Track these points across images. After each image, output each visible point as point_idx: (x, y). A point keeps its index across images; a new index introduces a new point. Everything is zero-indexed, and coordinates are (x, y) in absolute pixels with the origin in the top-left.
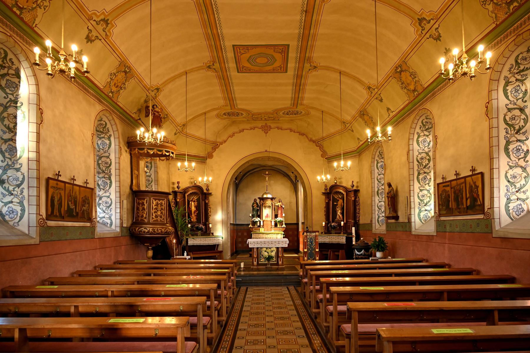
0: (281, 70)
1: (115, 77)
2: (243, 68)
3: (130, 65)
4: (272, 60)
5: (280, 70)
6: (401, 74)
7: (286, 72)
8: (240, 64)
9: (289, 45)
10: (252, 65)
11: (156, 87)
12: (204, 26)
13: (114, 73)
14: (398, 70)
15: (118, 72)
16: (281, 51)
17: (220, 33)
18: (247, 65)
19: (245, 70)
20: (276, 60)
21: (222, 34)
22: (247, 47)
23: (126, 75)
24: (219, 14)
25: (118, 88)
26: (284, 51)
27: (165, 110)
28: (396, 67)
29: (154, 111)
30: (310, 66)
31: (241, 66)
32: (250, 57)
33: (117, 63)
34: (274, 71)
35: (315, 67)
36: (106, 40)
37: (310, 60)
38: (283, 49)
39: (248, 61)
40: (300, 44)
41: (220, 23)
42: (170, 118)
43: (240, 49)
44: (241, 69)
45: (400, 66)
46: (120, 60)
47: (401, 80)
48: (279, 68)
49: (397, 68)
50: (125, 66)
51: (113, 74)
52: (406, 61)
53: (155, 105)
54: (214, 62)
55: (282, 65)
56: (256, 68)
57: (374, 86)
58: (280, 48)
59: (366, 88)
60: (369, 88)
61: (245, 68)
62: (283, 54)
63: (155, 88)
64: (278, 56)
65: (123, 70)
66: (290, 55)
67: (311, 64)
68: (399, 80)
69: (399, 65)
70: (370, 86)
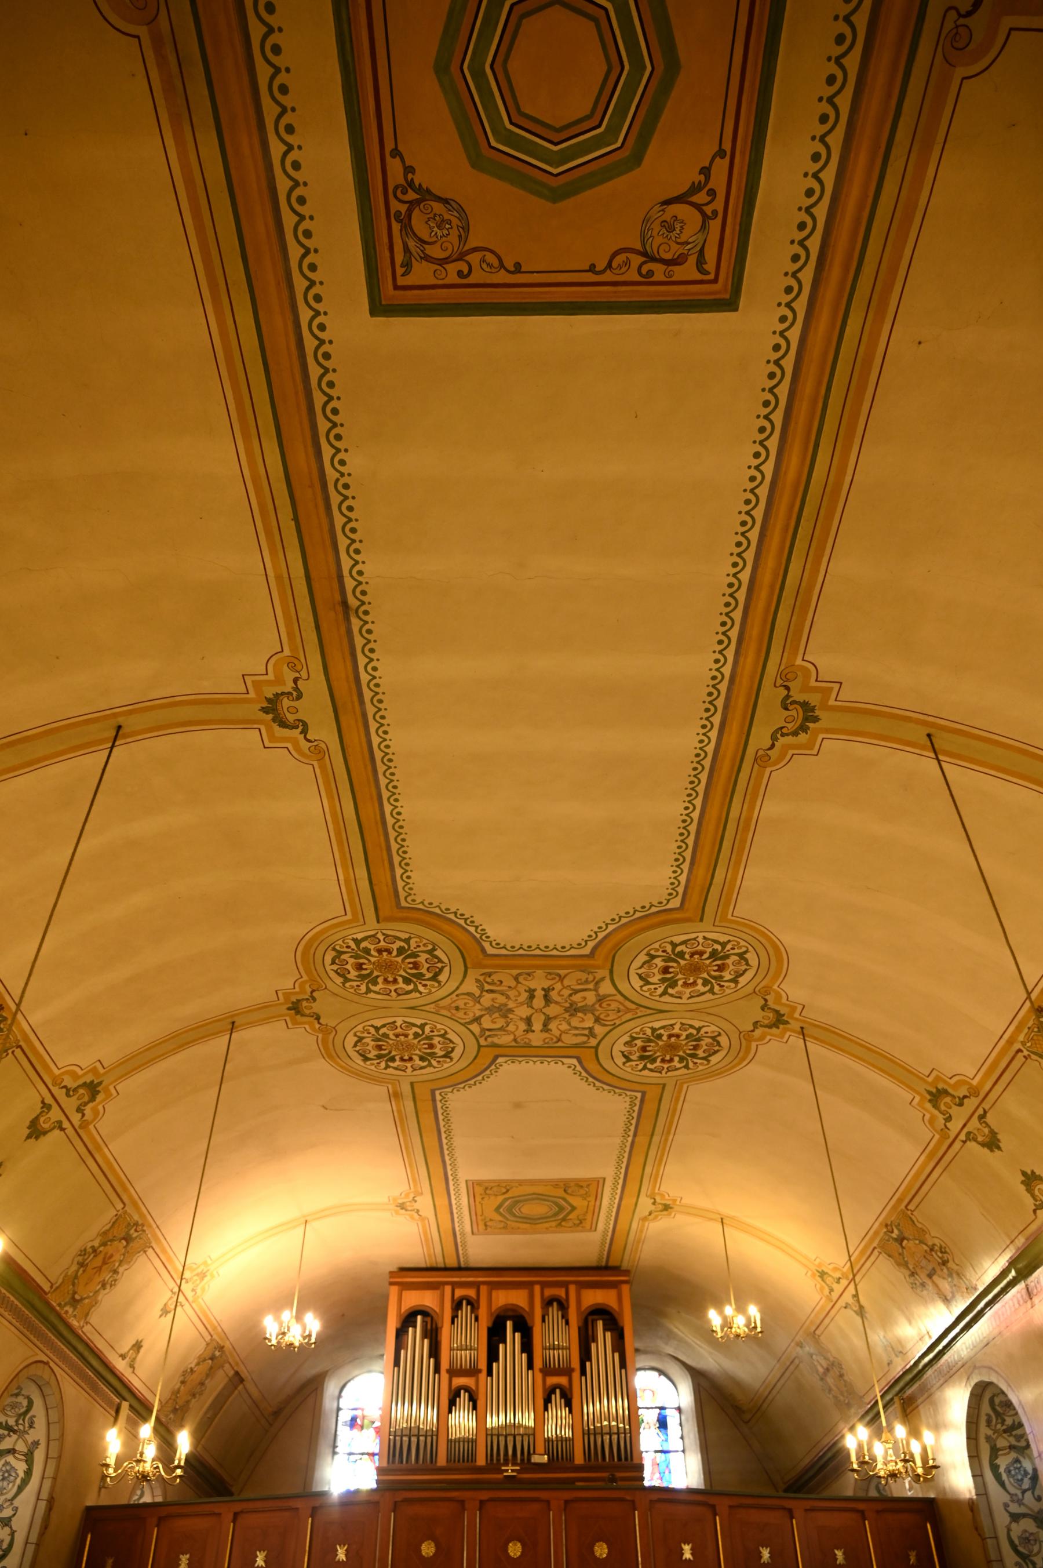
16: (418, 221)
26: (396, 227)
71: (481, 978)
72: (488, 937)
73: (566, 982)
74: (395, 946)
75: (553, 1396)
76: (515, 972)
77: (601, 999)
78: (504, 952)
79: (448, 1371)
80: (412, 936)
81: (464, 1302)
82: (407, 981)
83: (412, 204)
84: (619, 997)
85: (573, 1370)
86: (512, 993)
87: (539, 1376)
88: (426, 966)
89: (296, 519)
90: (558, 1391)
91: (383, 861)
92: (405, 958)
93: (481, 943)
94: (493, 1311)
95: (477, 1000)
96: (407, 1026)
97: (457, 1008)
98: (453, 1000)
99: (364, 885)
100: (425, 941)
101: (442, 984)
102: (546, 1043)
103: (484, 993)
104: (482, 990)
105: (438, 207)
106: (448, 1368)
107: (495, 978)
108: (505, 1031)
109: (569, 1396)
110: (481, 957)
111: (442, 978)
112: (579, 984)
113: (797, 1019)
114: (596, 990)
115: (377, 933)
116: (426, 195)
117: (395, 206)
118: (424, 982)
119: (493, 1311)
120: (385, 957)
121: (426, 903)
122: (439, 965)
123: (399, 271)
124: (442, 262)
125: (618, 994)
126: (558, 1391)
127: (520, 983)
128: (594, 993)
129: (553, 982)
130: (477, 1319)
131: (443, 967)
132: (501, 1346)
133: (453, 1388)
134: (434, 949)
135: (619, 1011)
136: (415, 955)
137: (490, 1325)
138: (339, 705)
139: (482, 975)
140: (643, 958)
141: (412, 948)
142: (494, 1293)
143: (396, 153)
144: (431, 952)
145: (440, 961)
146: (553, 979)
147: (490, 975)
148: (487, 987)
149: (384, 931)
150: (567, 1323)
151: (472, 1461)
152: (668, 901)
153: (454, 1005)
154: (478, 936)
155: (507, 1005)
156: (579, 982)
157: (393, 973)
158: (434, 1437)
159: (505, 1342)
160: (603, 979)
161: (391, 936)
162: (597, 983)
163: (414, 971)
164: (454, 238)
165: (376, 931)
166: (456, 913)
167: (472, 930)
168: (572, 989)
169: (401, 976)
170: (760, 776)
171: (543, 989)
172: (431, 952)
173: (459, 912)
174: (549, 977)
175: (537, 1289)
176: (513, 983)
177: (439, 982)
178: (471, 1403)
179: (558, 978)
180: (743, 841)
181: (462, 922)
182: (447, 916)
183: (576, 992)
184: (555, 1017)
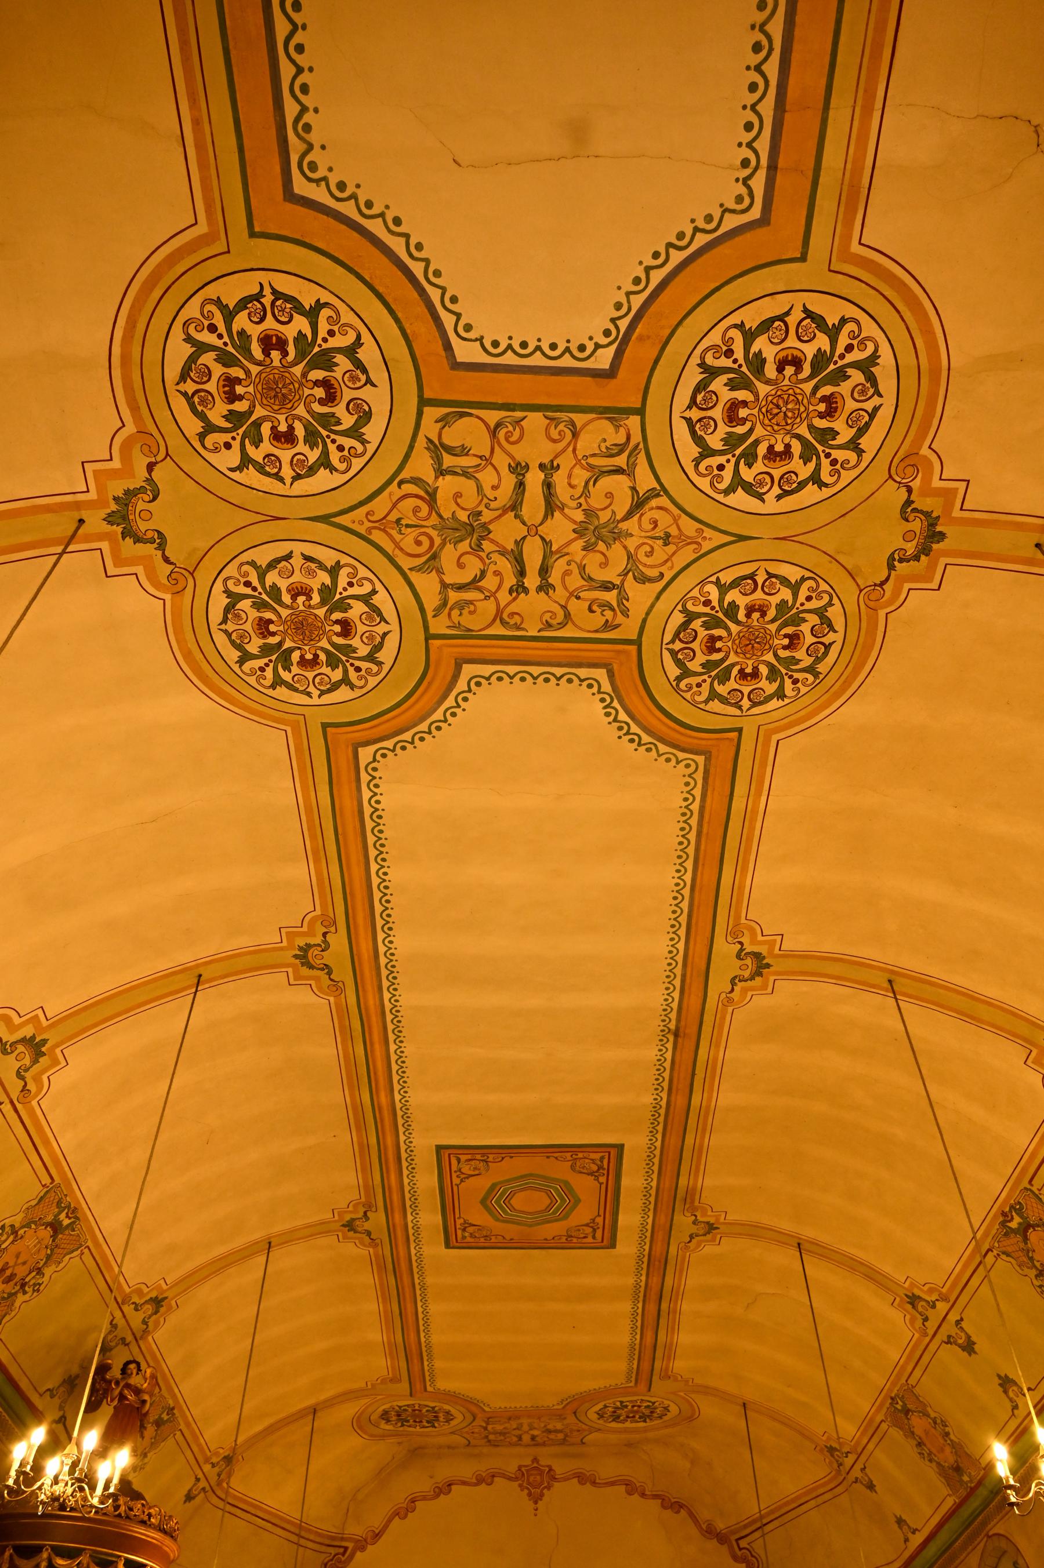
0: (594, 1237)
1: (12, 1242)
2: (464, 1230)
3: (78, 1202)
4: (562, 1198)
5: (590, 1239)
6: (1026, 1239)
7: (613, 1245)
8: (457, 1215)
9: (622, 1146)
10: (497, 1220)
11: (154, 1295)
12: (352, 1082)
13: (12, 1226)
14: (1014, 1225)
15: (28, 1225)
16: (595, 1168)
17: (398, 1105)
18: (478, 1217)
19: (471, 1235)
20: (580, 1200)
21: (405, 1107)
22: (485, 1154)
23: (54, 1236)
24: (401, 1042)
25: (12, 1283)
26: (606, 1166)
27: (170, 1390)
28: (1004, 1214)
29: (122, 1384)
30: (694, 1223)
31: (459, 1222)
32: (493, 1187)
33: (37, 1190)
34: (569, 1241)
35: (711, 1228)
36: (19, 1106)
37: (693, 1202)
38: (602, 1158)
39: (483, 1202)
40: (658, 1144)
41: (404, 1072)
42: (182, 1426)
43: (459, 1161)
44: (459, 1232)
45: (1018, 1208)
46: (46, 1180)
47: (1031, 1259)
48: (589, 1230)
49: (1006, 1216)
50: (59, 1202)
51: (7, 1229)
52: (1034, 1189)
53: (134, 1361)
54: (369, 1207)
55: (600, 1220)
56: (511, 1231)
57: (931, 1291)
58: (593, 1156)
59: (902, 1300)
60: (913, 1300)
61: (471, 1229)
62: (603, 1179)
63: (148, 1298)
64: (585, 1187)
65: (50, 1218)
66: (625, 1182)
67: (698, 1214)
68: (1025, 1259)
69: (1012, 1207)
70: (917, 1292)
71: (620, 618)
72: (603, 700)
73: (490, 607)
74: (732, 684)
76: (567, 632)
77: (432, 561)
78: (583, 672)
80: (702, 706)
82: (731, 611)
83: (597, 1172)
84: (406, 563)
86: (575, 581)
88: (695, 646)
89: (693, 1074)
91: (709, 823)
92: (723, 660)
93: (614, 690)
95: (633, 568)
96: (761, 484)
97: (667, 539)
98: (669, 564)
99: (741, 789)
100: (688, 696)
101: (680, 607)
102: (518, 422)
103: (617, 581)
104: (621, 588)
105: (585, 1171)
107: (598, 620)
108: (591, 467)
110: (615, 667)
111: (678, 618)
112: (471, 602)
113: (100, 537)
114: (444, 586)
115: (749, 709)
116: (591, 1174)
117: (605, 1172)
118: (707, 610)
120: (750, 663)
121: (673, 762)
122: (678, 646)
123: (607, 1157)
124: (585, 1158)
125: (408, 572)
127: (562, 606)
128: (448, 580)
129: (513, 608)
131: (673, 641)
134: (679, 679)
135: (398, 521)
136: (708, 666)
138: (702, 979)
139: (618, 626)
140: (386, 655)
141: (709, 680)
143: (601, 1184)
144: (686, 673)
145: (674, 654)
146: (512, 615)
147: (607, 626)
148: (611, 597)
149: (738, 712)
152: (374, 760)
153: (671, 548)
154: (616, 704)
155: (584, 549)
156: (472, 608)
157: (749, 627)
160: (437, 614)
161: (731, 705)
162: (445, 603)
163: (717, 632)
164: (578, 1164)
165: (749, 713)
166: (639, 744)
167: (623, 716)
168: (480, 589)
169: (738, 623)
170: (324, 905)
171: (526, 591)
172: (686, 673)
173: (635, 745)
174: (517, 619)
176: (574, 605)
177: (684, 611)
179: (505, 616)
180: (313, 837)
181: (634, 728)
182: (651, 740)
183: (473, 584)
184: (505, 511)
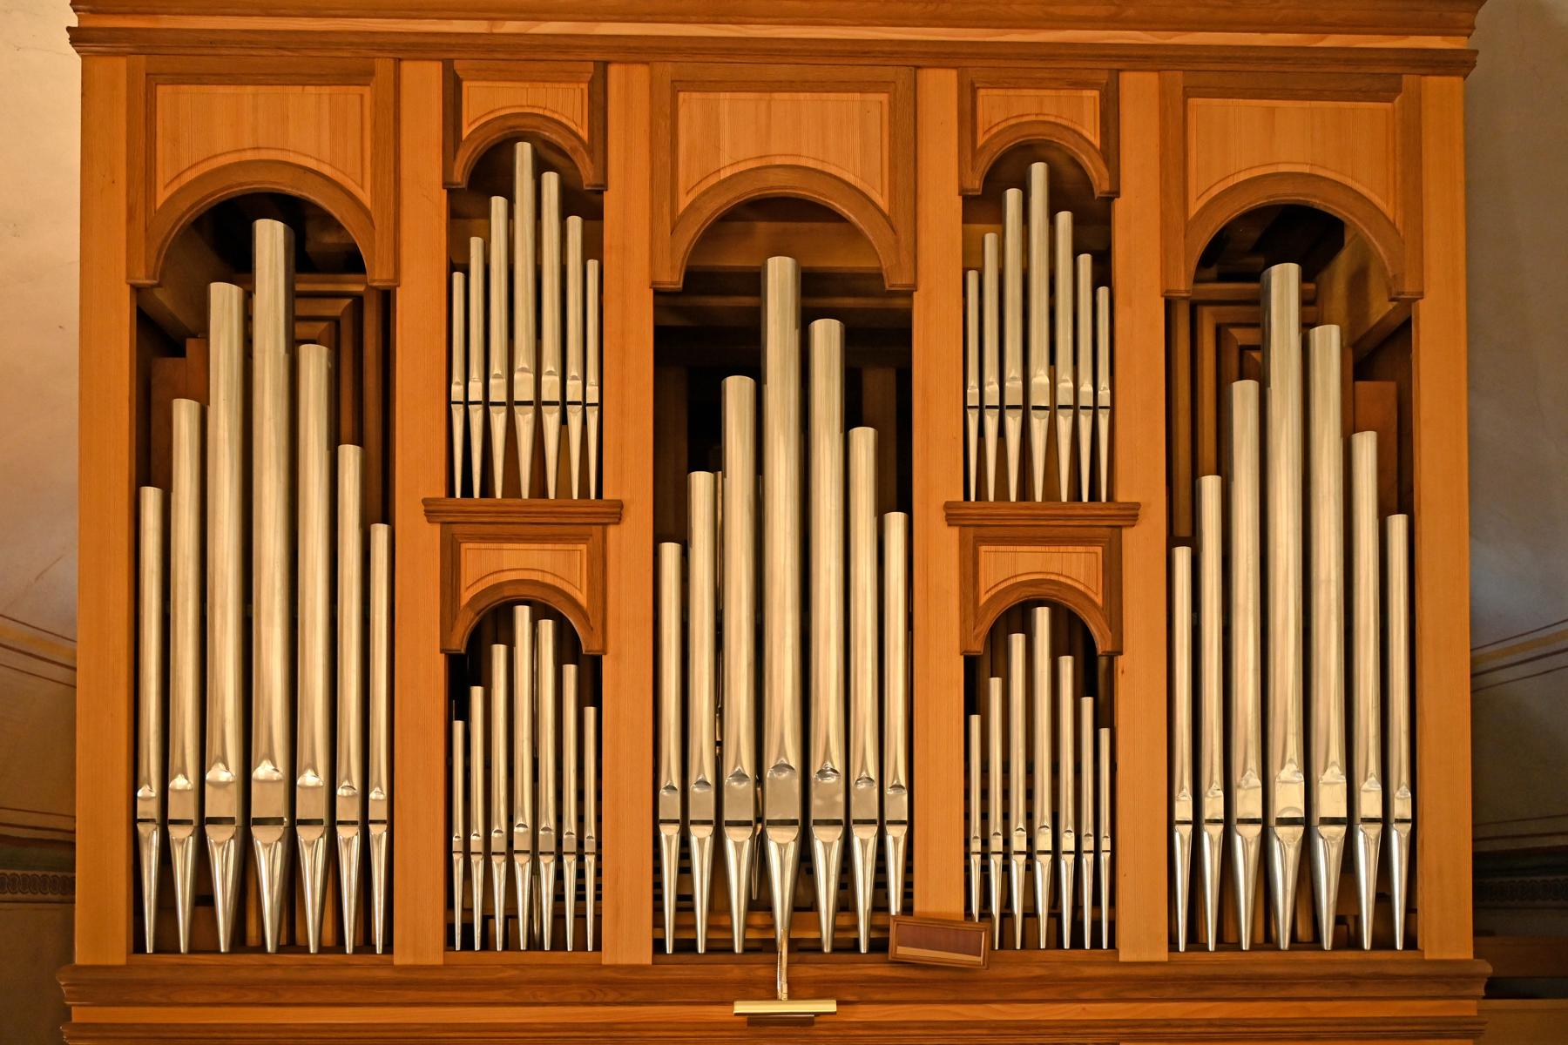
75: (1018, 641)
79: (431, 511)
81: (524, 151)
85: (1132, 514)
87: (943, 544)
90: (1042, 616)
94: (684, 202)
106: (441, 493)
109: (1103, 644)
119: (684, 202)
126: (1042, 616)
130: (593, 247)
132: (737, 389)
133: (466, 597)
137: (672, 278)
142: (691, 105)
150: (1103, 275)
151: (580, 945)
158: (378, 832)
159: (756, 371)
175: (940, 88)
178: (570, 671)
